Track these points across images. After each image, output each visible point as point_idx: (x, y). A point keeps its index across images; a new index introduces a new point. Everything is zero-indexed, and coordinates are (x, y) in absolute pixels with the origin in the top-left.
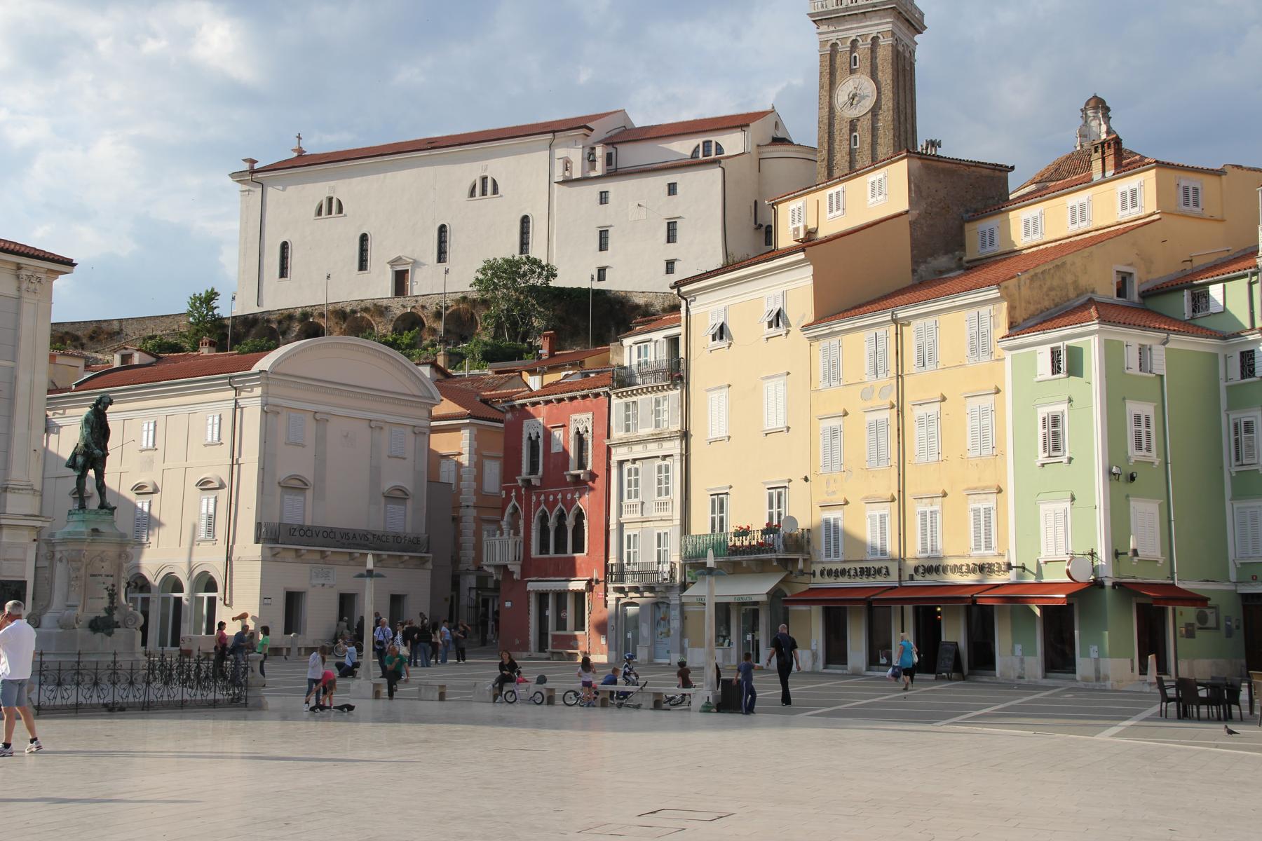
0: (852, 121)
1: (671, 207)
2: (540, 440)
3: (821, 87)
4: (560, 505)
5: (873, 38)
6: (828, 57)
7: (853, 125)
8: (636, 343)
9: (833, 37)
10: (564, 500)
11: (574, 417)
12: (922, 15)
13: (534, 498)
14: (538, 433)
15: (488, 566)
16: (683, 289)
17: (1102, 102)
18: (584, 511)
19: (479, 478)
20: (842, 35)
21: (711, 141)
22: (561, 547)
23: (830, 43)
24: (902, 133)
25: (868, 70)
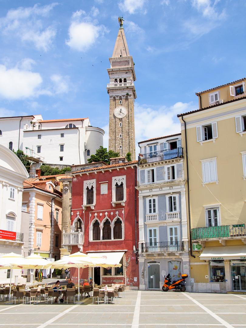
1: (62, 141)
2: (94, 189)
4: (107, 217)
7: (121, 120)
8: (148, 145)
9: (114, 95)
10: (109, 216)
11: (113, 178)
13: (90, 215)
14: (92, 186)
15: (65, 246)
16: (184, 117)
18: (121, 219)
19: (36, 212)
21: (72, 124)
22: (107, 235)
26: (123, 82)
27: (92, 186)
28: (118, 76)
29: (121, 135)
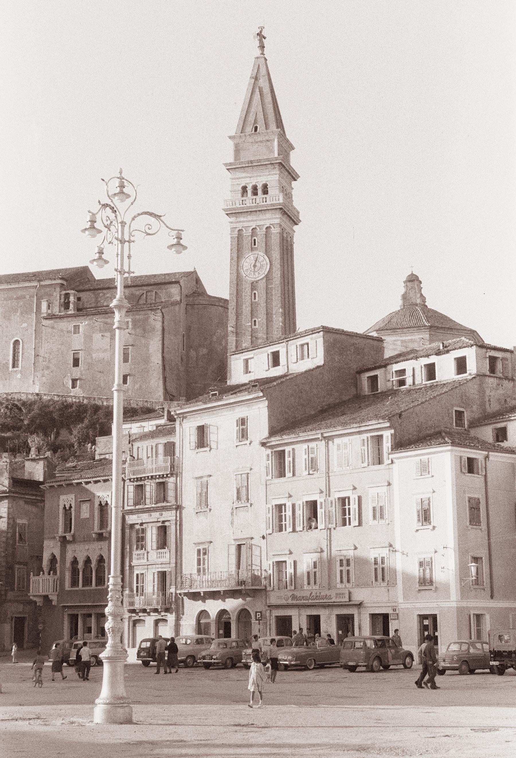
0: (253, 283)
2: (73, 509)
3: (232, 259)
5: (267, 228)
6: (236, 239)
7: (254, 286)
9: (240, 226)
12: (298, 213)
14: (71, 505)
15: (34, 596)
17: (417, 277)
20: (246, 224)
22: (87, 581)
23: (238, 229)
24: (286, 291)
25: (264, 249)
26: (260, 192)
27: (71, 505)
28: (248, 180)
29: (255, 321)
